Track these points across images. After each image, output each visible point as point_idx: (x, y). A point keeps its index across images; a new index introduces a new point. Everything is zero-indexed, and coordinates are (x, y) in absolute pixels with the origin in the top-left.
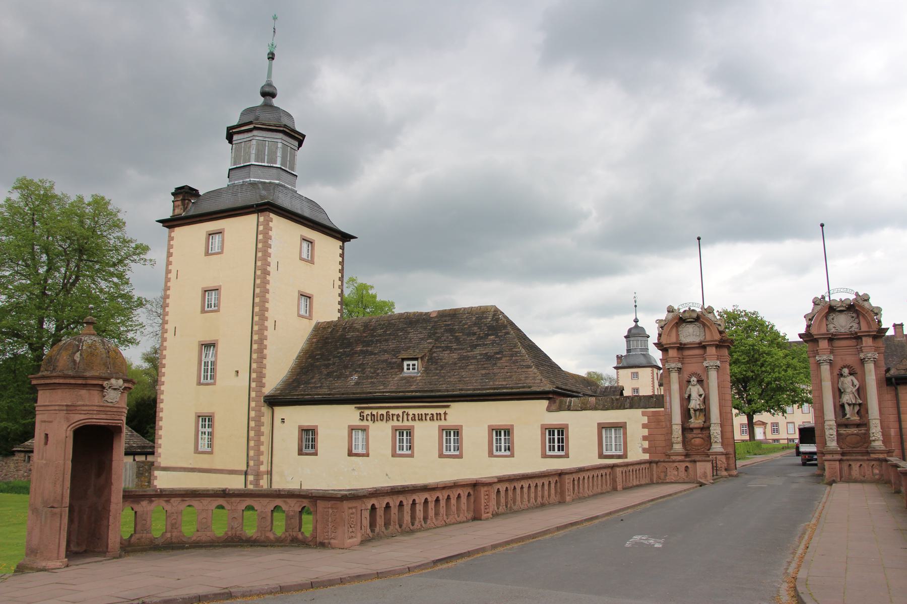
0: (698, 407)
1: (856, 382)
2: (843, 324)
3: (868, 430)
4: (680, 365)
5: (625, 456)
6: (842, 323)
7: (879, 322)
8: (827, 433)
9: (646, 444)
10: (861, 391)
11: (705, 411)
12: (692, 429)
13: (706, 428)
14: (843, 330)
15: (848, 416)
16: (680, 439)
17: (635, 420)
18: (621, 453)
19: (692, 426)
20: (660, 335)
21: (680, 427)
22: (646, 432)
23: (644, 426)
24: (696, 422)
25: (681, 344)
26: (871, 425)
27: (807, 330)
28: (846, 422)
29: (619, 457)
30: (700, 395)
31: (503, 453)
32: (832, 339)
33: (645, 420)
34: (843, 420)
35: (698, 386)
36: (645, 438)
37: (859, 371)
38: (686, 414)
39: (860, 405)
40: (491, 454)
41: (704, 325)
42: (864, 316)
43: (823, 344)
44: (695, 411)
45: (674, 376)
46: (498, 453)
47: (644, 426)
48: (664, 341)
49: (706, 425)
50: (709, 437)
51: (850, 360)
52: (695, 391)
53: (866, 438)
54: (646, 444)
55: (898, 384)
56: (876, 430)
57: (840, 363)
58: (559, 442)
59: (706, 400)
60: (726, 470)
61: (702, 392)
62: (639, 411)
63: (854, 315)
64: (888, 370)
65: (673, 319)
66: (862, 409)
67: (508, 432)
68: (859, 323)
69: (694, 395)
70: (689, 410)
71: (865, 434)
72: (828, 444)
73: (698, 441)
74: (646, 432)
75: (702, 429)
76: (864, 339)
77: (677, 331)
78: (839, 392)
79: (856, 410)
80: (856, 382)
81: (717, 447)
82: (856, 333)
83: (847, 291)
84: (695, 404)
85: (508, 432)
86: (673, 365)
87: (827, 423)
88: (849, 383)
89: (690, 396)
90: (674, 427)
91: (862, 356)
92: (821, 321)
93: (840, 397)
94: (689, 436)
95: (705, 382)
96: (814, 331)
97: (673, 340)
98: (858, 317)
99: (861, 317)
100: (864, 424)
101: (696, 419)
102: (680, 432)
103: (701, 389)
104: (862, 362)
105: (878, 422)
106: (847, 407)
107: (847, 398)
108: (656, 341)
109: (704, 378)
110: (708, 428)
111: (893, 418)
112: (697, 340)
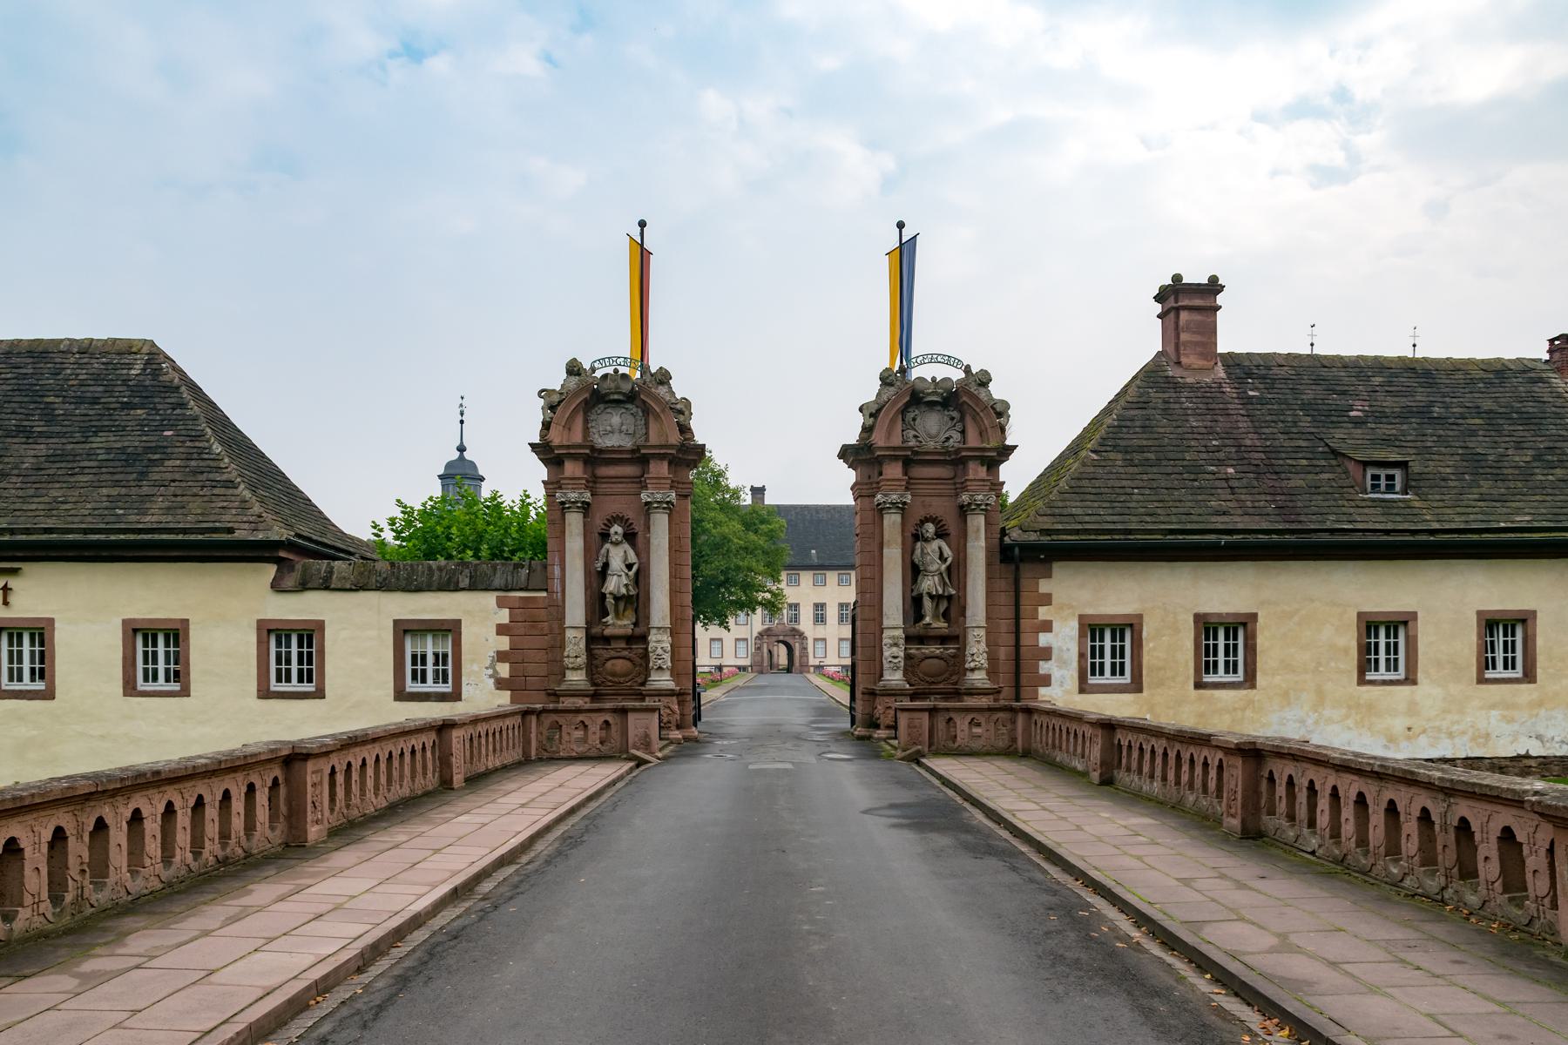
0: (624, 591)
1: (947, 552)
2: (934, 431)
3: (962, 650)
4: (587, 497)
5: (455, 696)
6: (932, 428)
7: (1003, 430)
8: (886, 653)
9: (504, 670)
10: (956, 572)
11: (636, 601)
12: (607, 640)
13: (638, 638)
14: (931, 445)
15: (928, 619)
16: (582, 660)
17: (481, 618)
18: (447, 688)
19: (608, 632)
20: (546, 426)
21: (581, 634)
22: (504, 643)
23: (501, 630)
24: (619, 624)
25: (593, 448)
26: (971, 639)
27: (861, 438)
28: (922, 632)
29: (442, 697)
30: (629, 567)
31: (161, 684)
32: (910, 460)
33: (504, 616)
34: (917, 629)
35: (626, 546)
36: (501, 656)
37: (952, 528)
38: (597, 604)
39: (950, 598)
40: (130, 689)
41: (647, 411)
42: (976, 417)
43: (894, 471)
44: (617, 598)
45: (574, 520)
46: (150, 687)
47: (501, 630)
48: (556, 437)
49: (638, 631)
50: (645, 656)
51: (941, 507)
52: (618, 556)
53: (957, 665)
54: (504, 670)
55: (1022, 560)
56: (977, 648)
57: (921, 513)
58: (300, 662)
59: (640, 577)
60: (679, 727)
61: (632, 557)
62: (490, 599)
63: (955, 414)
64: (1003, 532)
65: (577, 393)
66: (953, 606)
67: (176, 634)
68: (963, 432)
69: (616, 563)
70: (604, 595)
71: (954, 656)
72: (887, 676)
73: (620, 665)
74: (504, 643)
75: (630, 639)
76: (972, 465)
77: (586, 421)
78: (914, 571)
79: (942, 609)
80: (947, 552)
81: (662, 680)
82: (958, 451)
83: (949, 361)
84: (616, 583)
85: (176, 634)
86: (573, 496)
87: (886, 633)
88: (933, 551)
89: (606, 565)
90: (570, 634)
91: (965, 498)
92: (893, 421)
93: (915, 580)
94: (600, 651)
95: (640, 539)
96: (878, 439)
97: (577, 437)
98: (962, 419)
99: (968, 419)
100: (956, 638)
101: (617, 616)
102: (583, 645)
103: (631, 553)
104: (963, 511)
105: (982, 632)
106: (928, 604)
107: (929, 584)
108: (537, 440)
109: (638, 527)
110: (643, 638)
111: (1005, 625)
112: (628, 443)
